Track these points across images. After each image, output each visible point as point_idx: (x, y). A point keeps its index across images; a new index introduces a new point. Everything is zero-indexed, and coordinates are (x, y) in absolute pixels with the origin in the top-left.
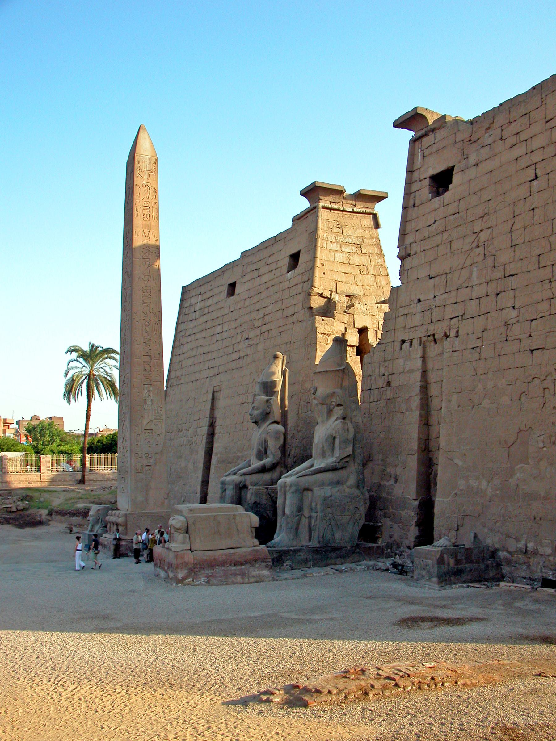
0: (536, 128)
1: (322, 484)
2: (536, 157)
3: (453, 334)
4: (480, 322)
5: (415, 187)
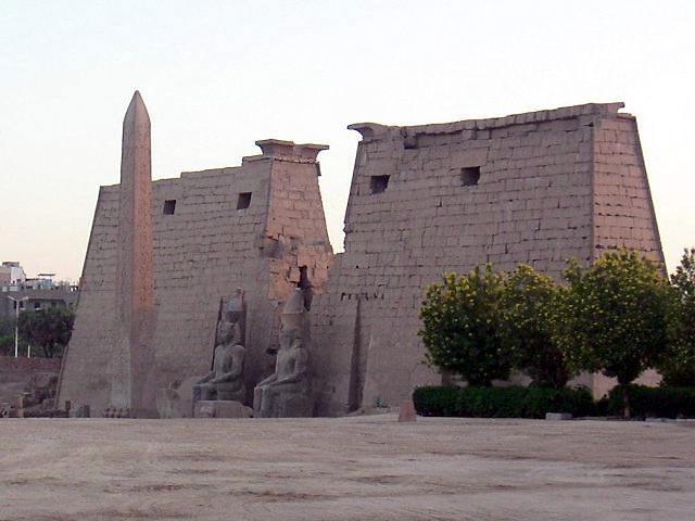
0: (444, 172)
1: (286, 391)
2: (443, 192)
3: (379, 296)
4: (398, 293)
5: (360, 180)
